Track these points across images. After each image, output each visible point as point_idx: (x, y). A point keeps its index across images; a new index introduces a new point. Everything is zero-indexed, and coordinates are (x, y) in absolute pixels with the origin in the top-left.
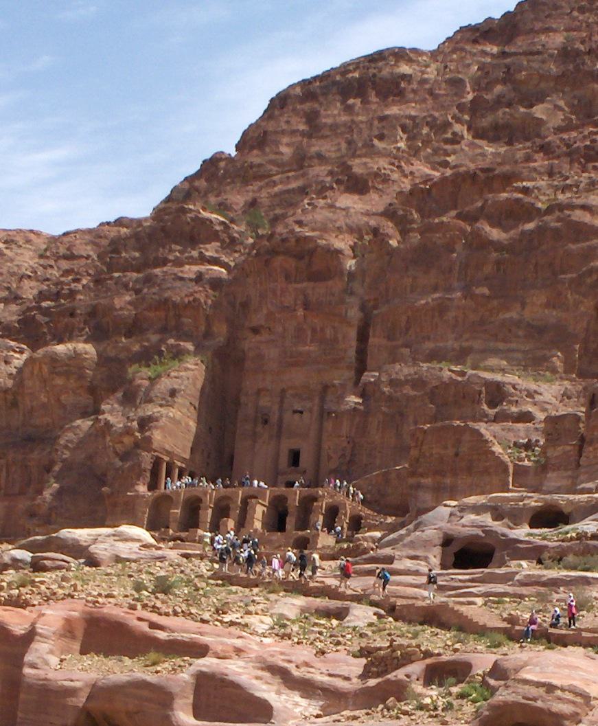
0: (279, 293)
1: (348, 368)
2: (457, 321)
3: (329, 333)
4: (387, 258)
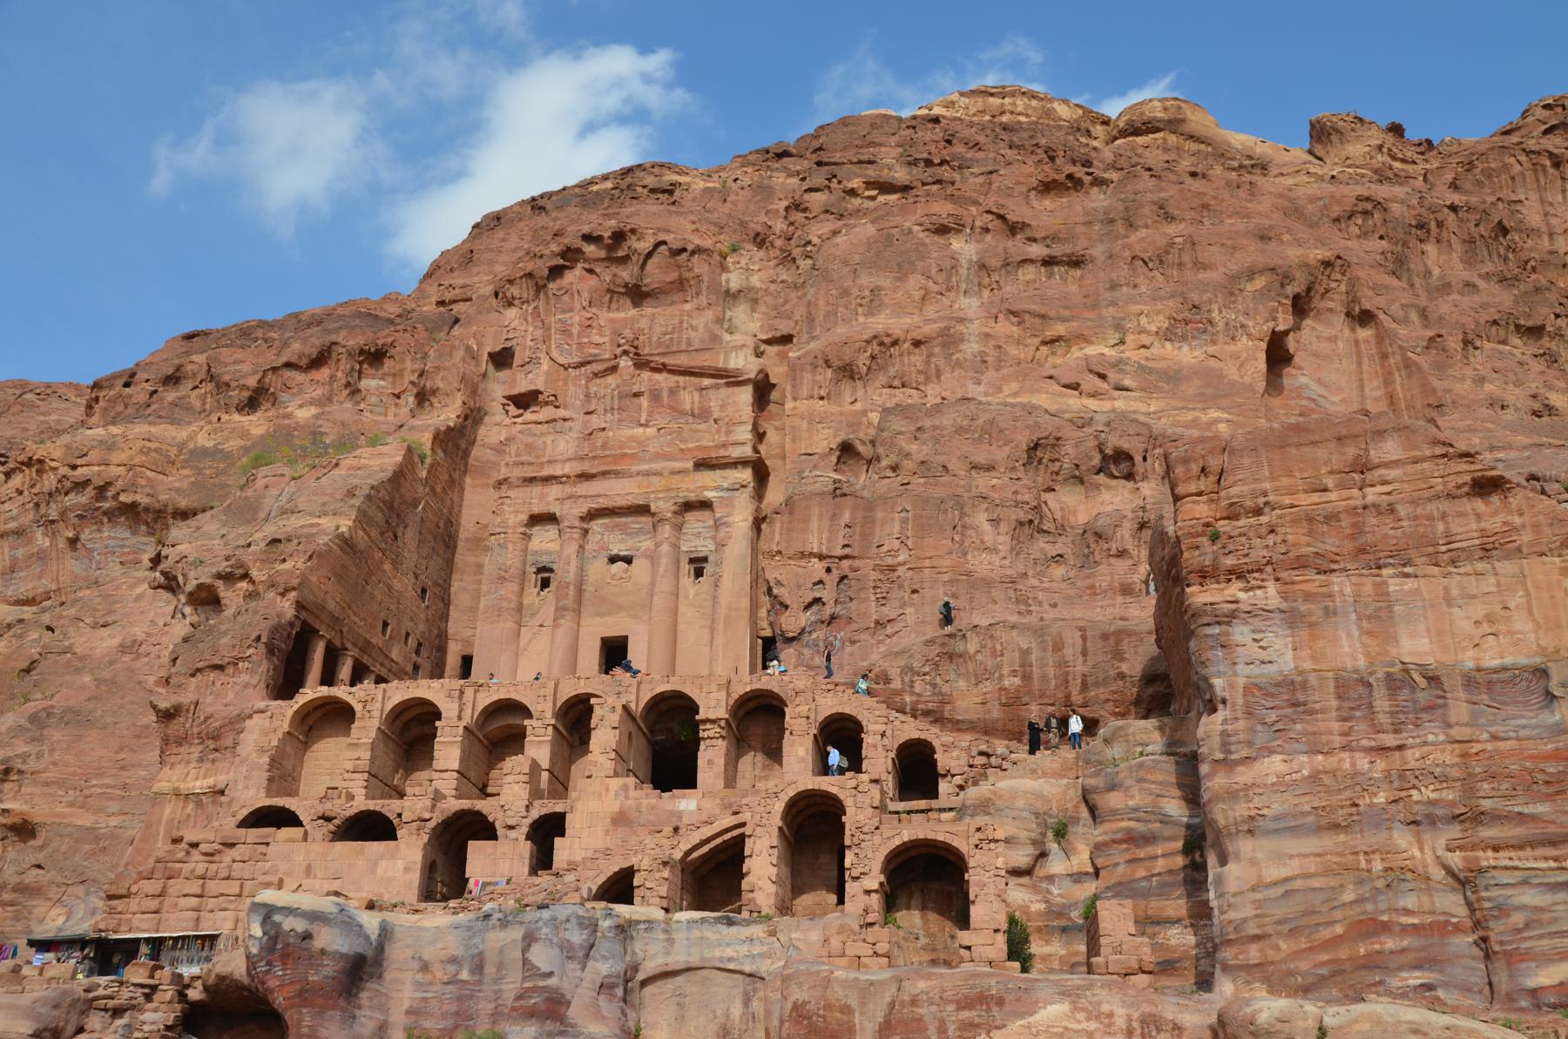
4: (805, 264)
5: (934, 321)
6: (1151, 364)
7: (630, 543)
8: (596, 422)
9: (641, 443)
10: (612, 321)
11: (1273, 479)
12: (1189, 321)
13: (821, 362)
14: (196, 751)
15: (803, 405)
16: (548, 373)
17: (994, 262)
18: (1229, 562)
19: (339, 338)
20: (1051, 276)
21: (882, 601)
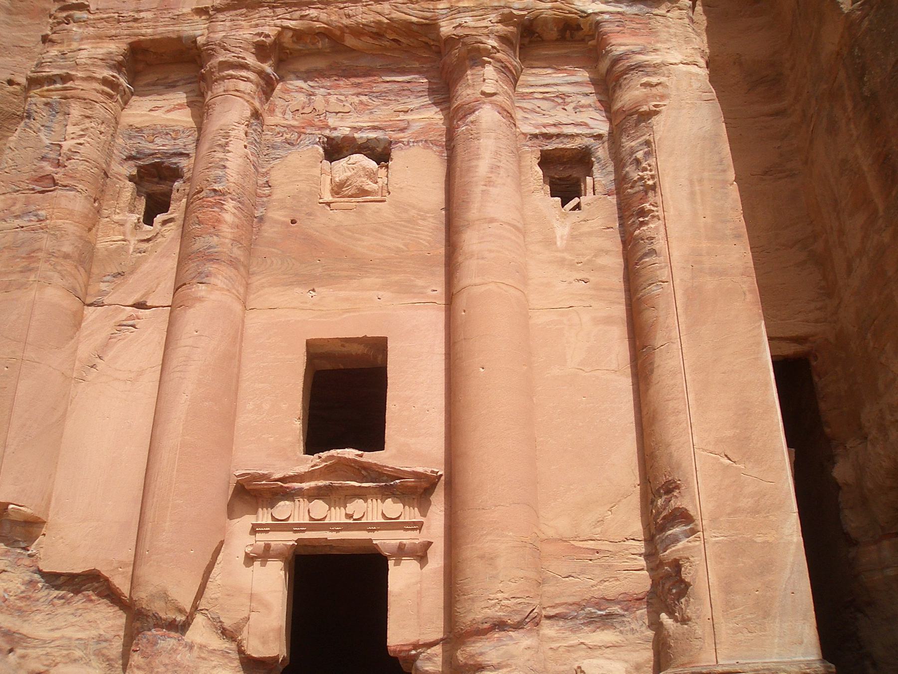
7: (383, 113)
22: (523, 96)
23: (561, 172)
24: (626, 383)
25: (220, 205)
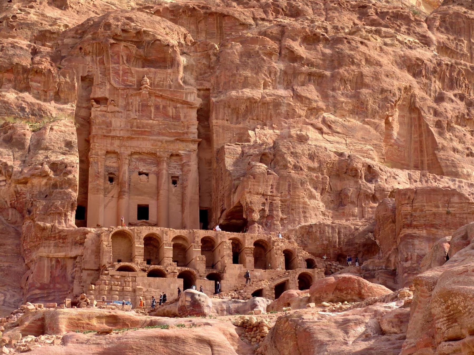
0: (121, 73)
1: (193, 141)
2: (288, 114)
3: (171, 111)
5: (271, 96)
6: (346, 123)
7: (147, 167)
8: (133, 115)
9: (152, 126)
10: (137, 72)
11: (427, 203)
12: (360, 110)
13: (227, 105)
14: (52, 242)
15: (220, 122)
16: (109, 90)
17: (290, 72)
18: (415, 223)
19: (16, 60)
20: (310, 80)
21: (283, 212)
22: (169, 166)
23: (174, 179)
24: (180, 213)
25: (125, 183)
